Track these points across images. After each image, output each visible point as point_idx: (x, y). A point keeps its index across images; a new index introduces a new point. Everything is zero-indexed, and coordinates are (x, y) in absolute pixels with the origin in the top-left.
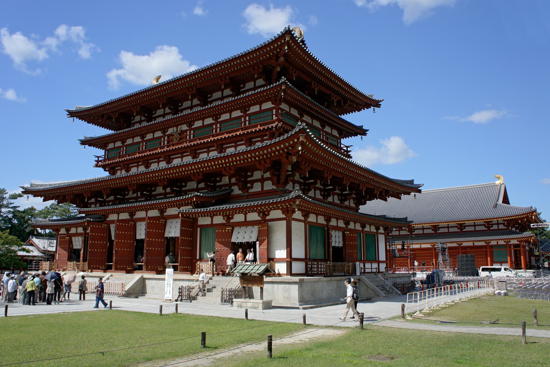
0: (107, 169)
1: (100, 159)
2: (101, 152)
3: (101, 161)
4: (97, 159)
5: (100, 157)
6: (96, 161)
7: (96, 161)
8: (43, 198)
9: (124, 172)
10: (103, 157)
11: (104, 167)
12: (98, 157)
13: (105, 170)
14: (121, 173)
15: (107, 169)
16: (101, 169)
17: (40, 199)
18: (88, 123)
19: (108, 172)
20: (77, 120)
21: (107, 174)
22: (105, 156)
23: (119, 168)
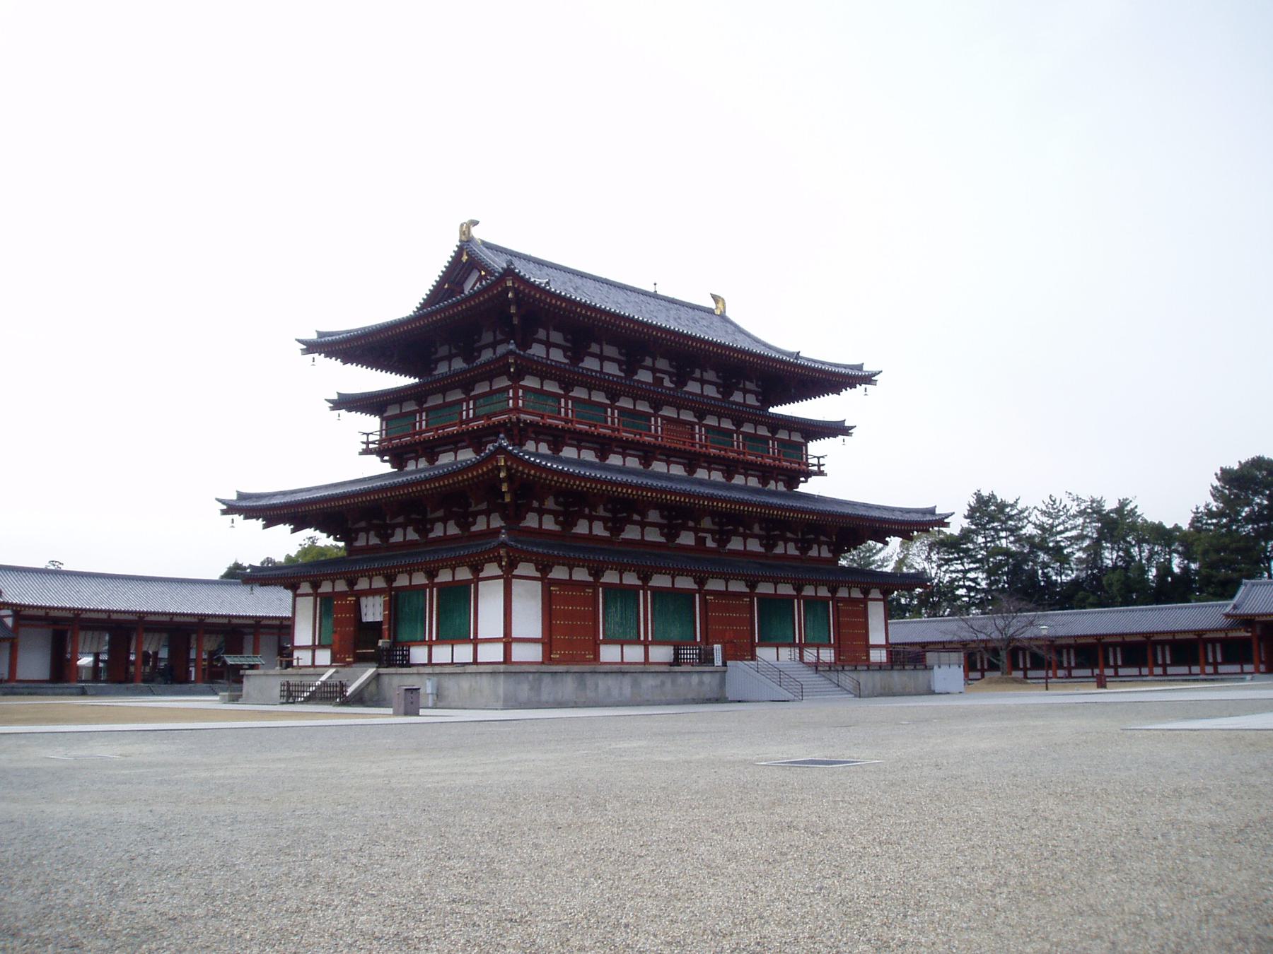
1: (372, 438)
2: (372, 424)
3: (373, 443)
4: (364, 438)
7: (363, 443)
8: (292, 527)
9: (423, 464)
10: (378, 433)
11: (380, 453)
12: (368, 435)
14: (417, 468)
17: (284, 529)
18: (345, 362)
19: (388, 465)
20: (320, 358)
21: (387, 468)
22: (381, 431)
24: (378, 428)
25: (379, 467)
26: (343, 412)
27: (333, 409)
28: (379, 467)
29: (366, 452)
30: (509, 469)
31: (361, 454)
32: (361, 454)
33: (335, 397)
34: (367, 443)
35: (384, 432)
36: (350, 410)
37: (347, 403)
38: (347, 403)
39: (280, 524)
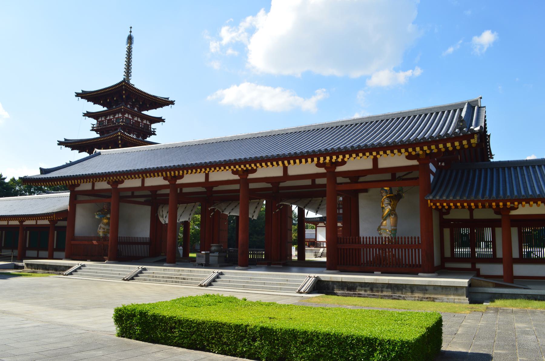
0: (98, 133)
1: (95, 126)
2: (95, 122)
3: (95, 127)
4: (92, 126)
5: (95, 125)
6: (92, 127)
11: (96, 131)
12: (93, 125)
13: (97, 133)
15: (98, 133)
16: (94, 132)
21: (98, 136)
22: (97, 124)
23: (111, 131)
24: (96, 123)
25: (95, 135)
26: (87, 117)
27: (83, 116)
28: (95, 135)
29: (92, 130)
30: (121, 137)
31: (91, 130)
32: (91, 130)
33: (86, 112)
34: (93, 127)
35: (98, 124)
36: (89, 117)
37: (88, 115)
38: (88, 115)
39: (84, 152)
